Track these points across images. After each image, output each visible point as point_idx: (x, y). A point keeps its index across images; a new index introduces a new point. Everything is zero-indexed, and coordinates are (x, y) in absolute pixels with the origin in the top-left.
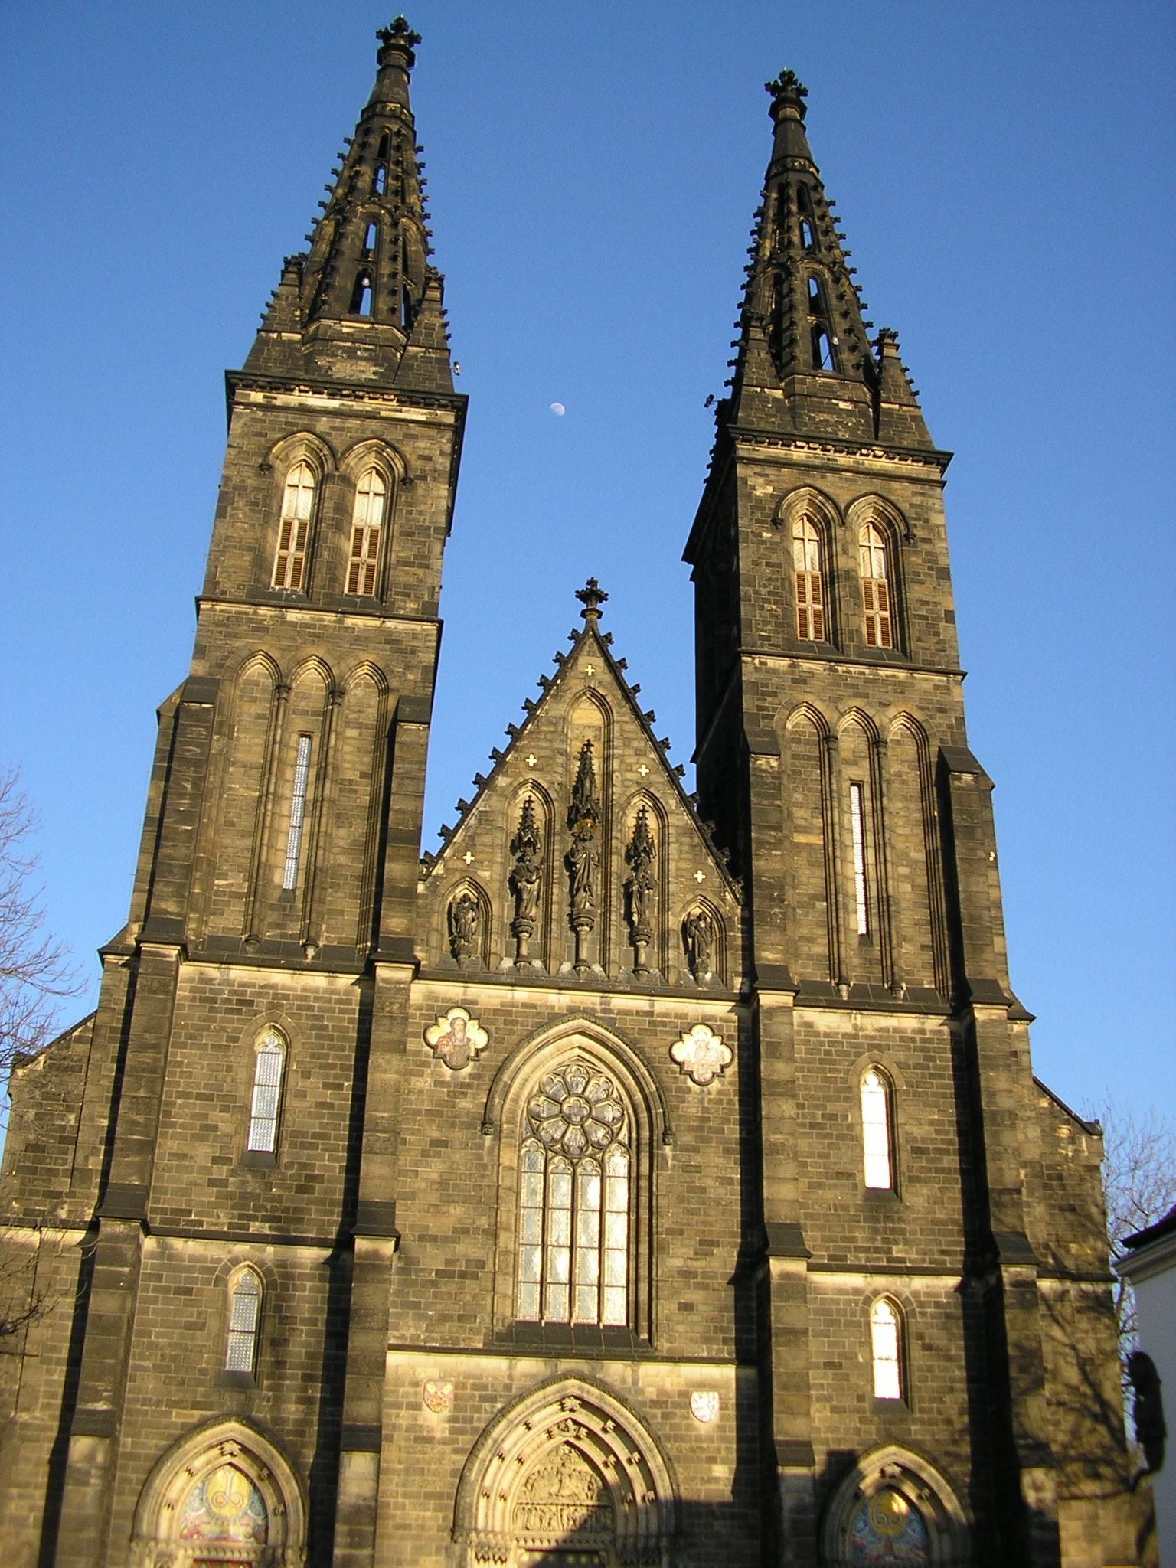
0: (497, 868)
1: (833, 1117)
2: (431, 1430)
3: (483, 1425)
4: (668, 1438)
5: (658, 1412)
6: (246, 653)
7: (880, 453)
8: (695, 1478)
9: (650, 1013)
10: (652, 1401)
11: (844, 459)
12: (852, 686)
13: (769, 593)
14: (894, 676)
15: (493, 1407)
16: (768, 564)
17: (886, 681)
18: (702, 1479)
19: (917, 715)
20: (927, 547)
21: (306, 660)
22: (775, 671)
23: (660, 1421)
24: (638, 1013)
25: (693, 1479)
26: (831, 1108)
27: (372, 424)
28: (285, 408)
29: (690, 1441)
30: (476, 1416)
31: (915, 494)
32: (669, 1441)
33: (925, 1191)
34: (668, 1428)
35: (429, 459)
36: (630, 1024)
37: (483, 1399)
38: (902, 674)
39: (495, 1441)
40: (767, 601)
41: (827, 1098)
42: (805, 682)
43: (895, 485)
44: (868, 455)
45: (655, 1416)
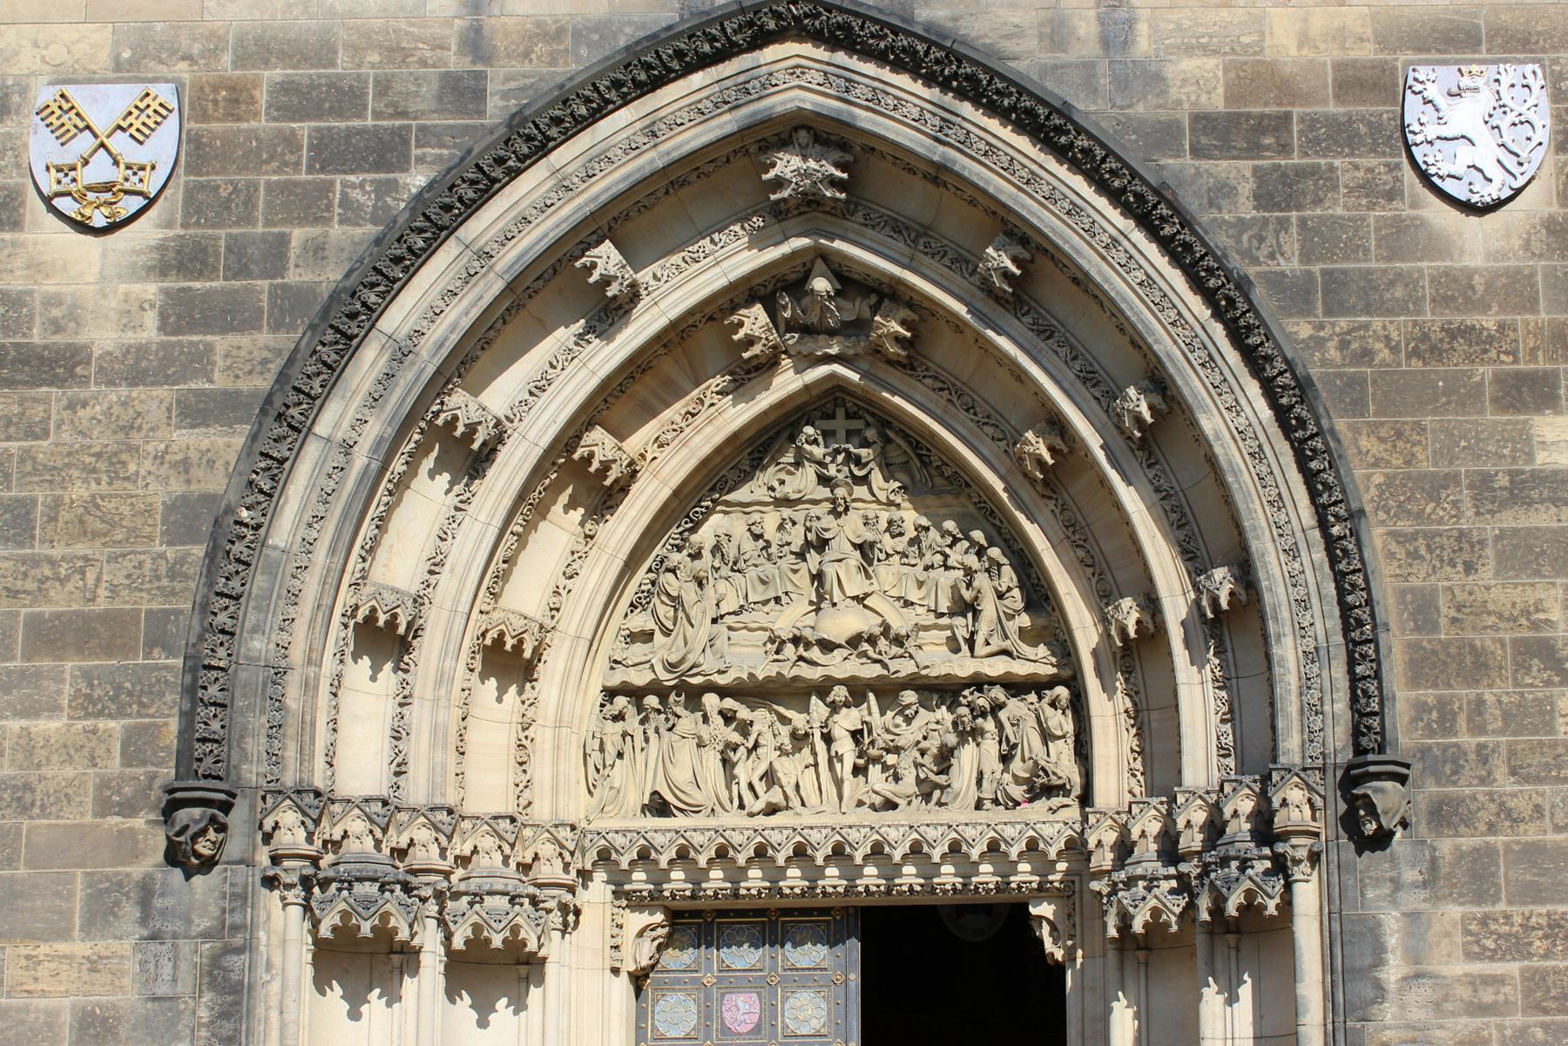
2: (74, 315)
3: (331, 275)
4: (1298, 295)
5: (1239, 172)
8: (1454, 478)
10: (1204, 121)
15: (392, 186)
18: (1483, 483)
23: (1247, 210)
25: (1436, 486)
29: (1411, 304)
30: (298, 235)
32: (1305, 309)
34: (1291, 242)
37: (330, 154)
39: (402, 354)
45: (1222, 192)
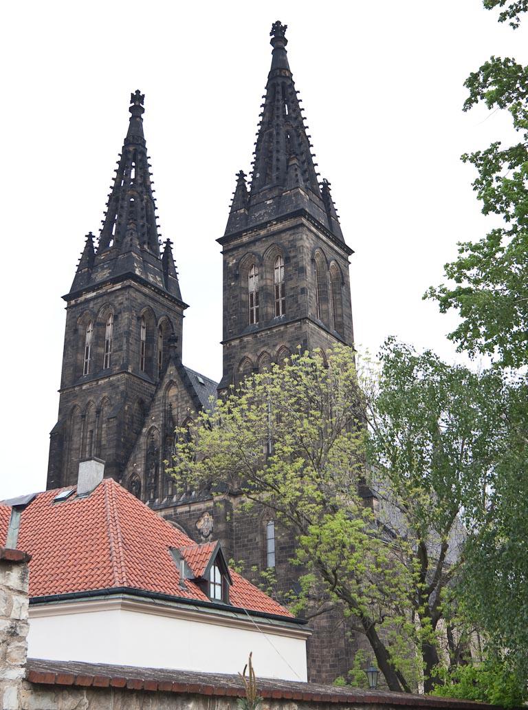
0: (143, 466)
1: (251, 540)
6: (72, 407)
7: (275, 223)
9: (189, 511)
11: (262, 233)
12: (264, 341)
13: (233, 311)
14: (279, 330)
16: (233, 298)
17: (275, 335)
19: (288, 345)
20: (295, 260)
21: (89, 403)
22: (235, 346)
24: (186, 512)
26: (251, 536)
27: (106, 297)
28: (81, 303)
31: (291, 235)
33: (284, 566)
35: (122, 303)
36: (183, 518)
38: (282, 328)
40: (232, 315)
41: (249, 533)
42: (245, 347)
43: (283, 235)
44: (272, 225)
